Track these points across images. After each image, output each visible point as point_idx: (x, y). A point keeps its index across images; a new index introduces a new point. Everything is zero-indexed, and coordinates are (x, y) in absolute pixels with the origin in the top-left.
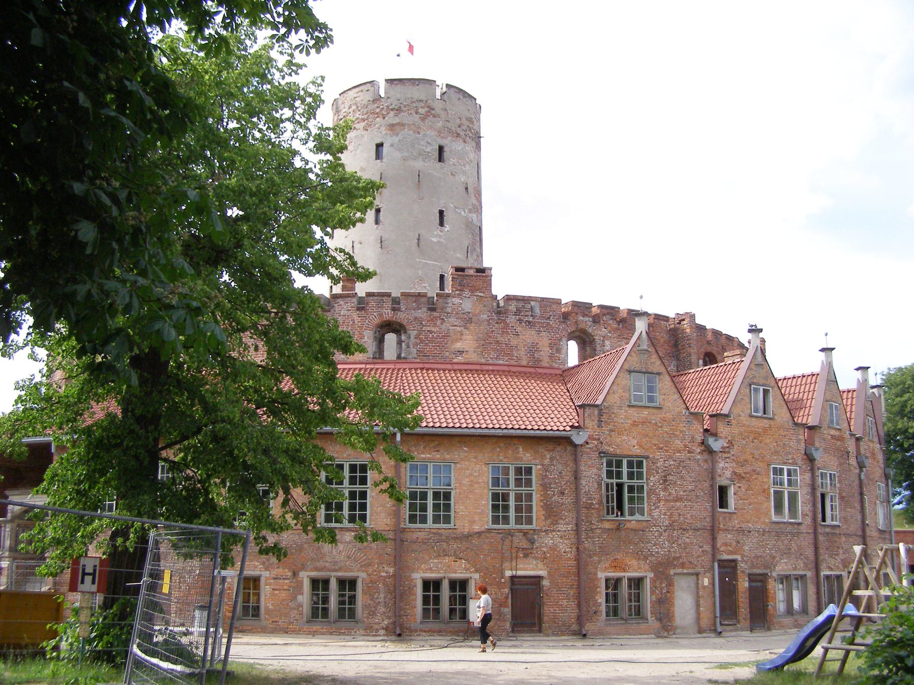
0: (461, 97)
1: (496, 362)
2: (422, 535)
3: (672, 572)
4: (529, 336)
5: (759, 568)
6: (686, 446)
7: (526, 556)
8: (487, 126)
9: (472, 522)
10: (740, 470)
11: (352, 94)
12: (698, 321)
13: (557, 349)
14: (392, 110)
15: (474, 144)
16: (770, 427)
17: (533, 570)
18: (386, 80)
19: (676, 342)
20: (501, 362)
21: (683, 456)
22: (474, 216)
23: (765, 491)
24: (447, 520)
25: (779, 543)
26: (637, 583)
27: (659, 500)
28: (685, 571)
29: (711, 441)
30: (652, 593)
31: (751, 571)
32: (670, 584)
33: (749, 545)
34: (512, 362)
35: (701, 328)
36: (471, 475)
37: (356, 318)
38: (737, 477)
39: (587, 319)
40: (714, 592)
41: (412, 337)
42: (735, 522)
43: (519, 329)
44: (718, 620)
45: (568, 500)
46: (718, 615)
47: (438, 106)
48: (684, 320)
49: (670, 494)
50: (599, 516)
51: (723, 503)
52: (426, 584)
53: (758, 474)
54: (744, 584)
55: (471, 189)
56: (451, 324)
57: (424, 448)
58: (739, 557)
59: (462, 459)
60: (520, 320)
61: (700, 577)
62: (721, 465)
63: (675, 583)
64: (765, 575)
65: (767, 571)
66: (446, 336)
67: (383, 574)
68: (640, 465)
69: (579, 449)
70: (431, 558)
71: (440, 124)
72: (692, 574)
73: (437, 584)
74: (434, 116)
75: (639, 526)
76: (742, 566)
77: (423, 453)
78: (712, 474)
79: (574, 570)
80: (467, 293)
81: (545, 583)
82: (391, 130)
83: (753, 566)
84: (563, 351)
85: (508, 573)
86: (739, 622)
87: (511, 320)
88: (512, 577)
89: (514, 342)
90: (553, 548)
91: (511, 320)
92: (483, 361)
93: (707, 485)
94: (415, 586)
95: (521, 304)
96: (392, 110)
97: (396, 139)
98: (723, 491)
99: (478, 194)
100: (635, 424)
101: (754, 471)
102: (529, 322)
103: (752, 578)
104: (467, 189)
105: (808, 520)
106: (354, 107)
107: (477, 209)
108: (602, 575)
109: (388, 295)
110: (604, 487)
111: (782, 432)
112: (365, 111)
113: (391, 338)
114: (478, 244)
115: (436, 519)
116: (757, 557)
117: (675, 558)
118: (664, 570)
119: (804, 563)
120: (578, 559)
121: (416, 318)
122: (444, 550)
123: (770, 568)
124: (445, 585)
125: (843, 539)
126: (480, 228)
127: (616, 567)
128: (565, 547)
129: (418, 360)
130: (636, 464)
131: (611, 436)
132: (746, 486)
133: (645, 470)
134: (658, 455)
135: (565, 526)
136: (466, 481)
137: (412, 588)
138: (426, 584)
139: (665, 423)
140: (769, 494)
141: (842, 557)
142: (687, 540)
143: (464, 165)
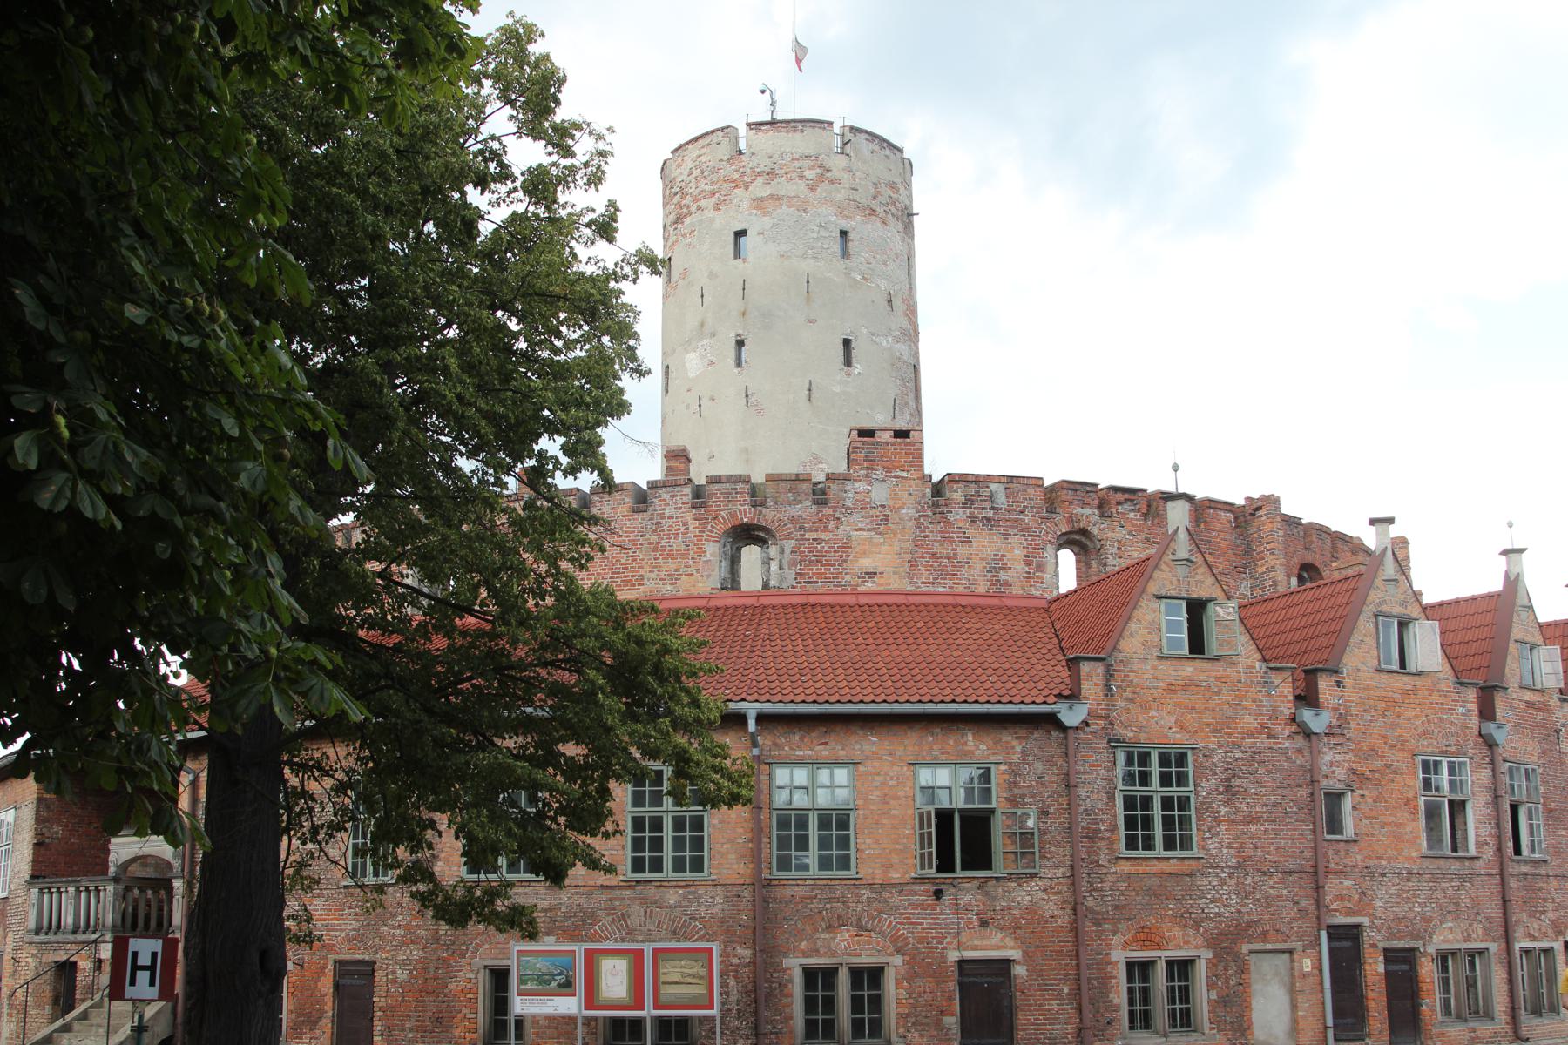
0: (877, 148)
1: (932, 589)
2: (800, 891)
3: (1245, 948)
4: (986, 544)
5: (1401, 938)
6: (1263, 726)
7: (984, 924)
8: (924, 197)
9: (888, 866)
10: (1363, 767)
11: (693, 151)
12: (1286, 509)
13: (1037, 566)
14: (759, 174)
15: (900, 226)
16: (1415, 690)
17: (998, 948)
18: (749, 125)
19: (1248, 546)
20: (941, 590)
21: (1262, 741)
22: (903, 348)
24: (844, 863)
25: (1438, 893)
26: (1181, 969)
27: (1218, 821)
28: (1269, 946)
29: (1307, 715)
30: (1211, 986)
31: (1388, 945)
32: (1243, 970)
33: (1383, 899)
34: (961, 589)
35: (1292, 522)
36: (884, 784)
37: (689, 516)
38: (1357, 779)
39: (1088, 511)
40: (1322, 984)
41: (788, 551)
42: (1357, 858)
43: (971, 532)
44: (1330, 1033)
45: (1055, 825)
46: (1330, 1023)
47: (837, 163)
48: (1260, 508)
49: (1238, 811)
50: (1112, 851)
51: (1334, 825)
52: (810, 975)
53: (1395, 772)
54: (1375, 968)
55: (897, 303)
56: (853, 528)
57: (802, 739)
58: (1365, 921)
59: (867, 758)
60: (973, 518)
61: (1296, 956)
62: (1328, 758)
63: (1252, 968)
64: (1417, 949)
65: (1419, 944)
66: (847, 546)
67: (735, 961)
68: (1182, 759)
69: (1071, 734)
70: (816, 930)
71: (840, 196)
72: (1283, 952)
73: (829, 974)
74: (832, 182)
75: (1187, 866)
76: (1370, 935)
77: (800, 748)
78: (1311, 775)
79: (1068, 948)
80: (879, 473)
81: (1019, 971)
82: (759, 208)
83: (1392, 936)
84: (1050, 568)
85: (953, 956)
87: (958, 516)
88: (962, 962)
89: (962, 552)
90: (1031, 910)
91: (958, 516)
92: (910, 588)
93: (1303, 793)
94: (791, 981)
95: (973, 489)
96: (759, 174)
97: (767, 222)
98: (1334, 798)
99: (911, 312)
100: (1171, 689)
101: (1388, 766)
102: (989, 520)
103: (1391, 956)
104: (890, 302)
105: (1489, 853)
106: (697, 172)
107: (911, 335)
108: (1119, 956)
109: (745, 480)
110: (1119, 802)
111: (1435, 697)
112: (715, 177)
113: (751, 555)
114: (912, 395)
115: (825, 863)
116: (1398, 919)
117: (1249, 924)
118: (1229, 944)
119: (1485, 929)
120: (1075, 929)
121: (792, 519)
122: (839, 917)
123: (1422, 938)
124: (844, 978)
125: (1553, 883)
126: (916, 368)
127: (1146, 938)
128: (1052, 907)
129: (798, 590)
130: (1175, 764)
131: (1127, 710)
132: (1375, 794)
133: (1190, 769)
134: (1212, 743)
135: (1053, 872)
136: (875, 795)
137: (784, 985)
138: (810, 975)
139: (1225, 687)
140: (1416, 807)
141: (1551, 915)
142: (1272, 892)
143: (885, 263)
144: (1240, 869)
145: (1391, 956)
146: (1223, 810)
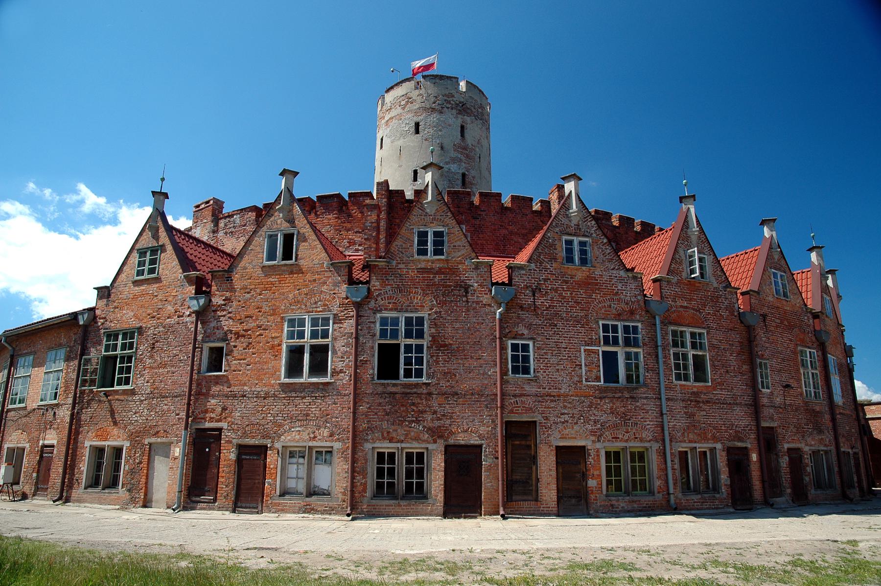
5: (253, 437)
23: (275, 349)
25: (291, 408)
26: (118, 451)
27: (145, 368)
30: (127, 462)
31: (240, 441)
49: (156, 361)
54: (229, 455)
58: (224, 425)
86: (215, 500)
103: (242, 449)
108: (87, 444)
144: (151, 395)
145: (242, 449)
146: (148, 361)
